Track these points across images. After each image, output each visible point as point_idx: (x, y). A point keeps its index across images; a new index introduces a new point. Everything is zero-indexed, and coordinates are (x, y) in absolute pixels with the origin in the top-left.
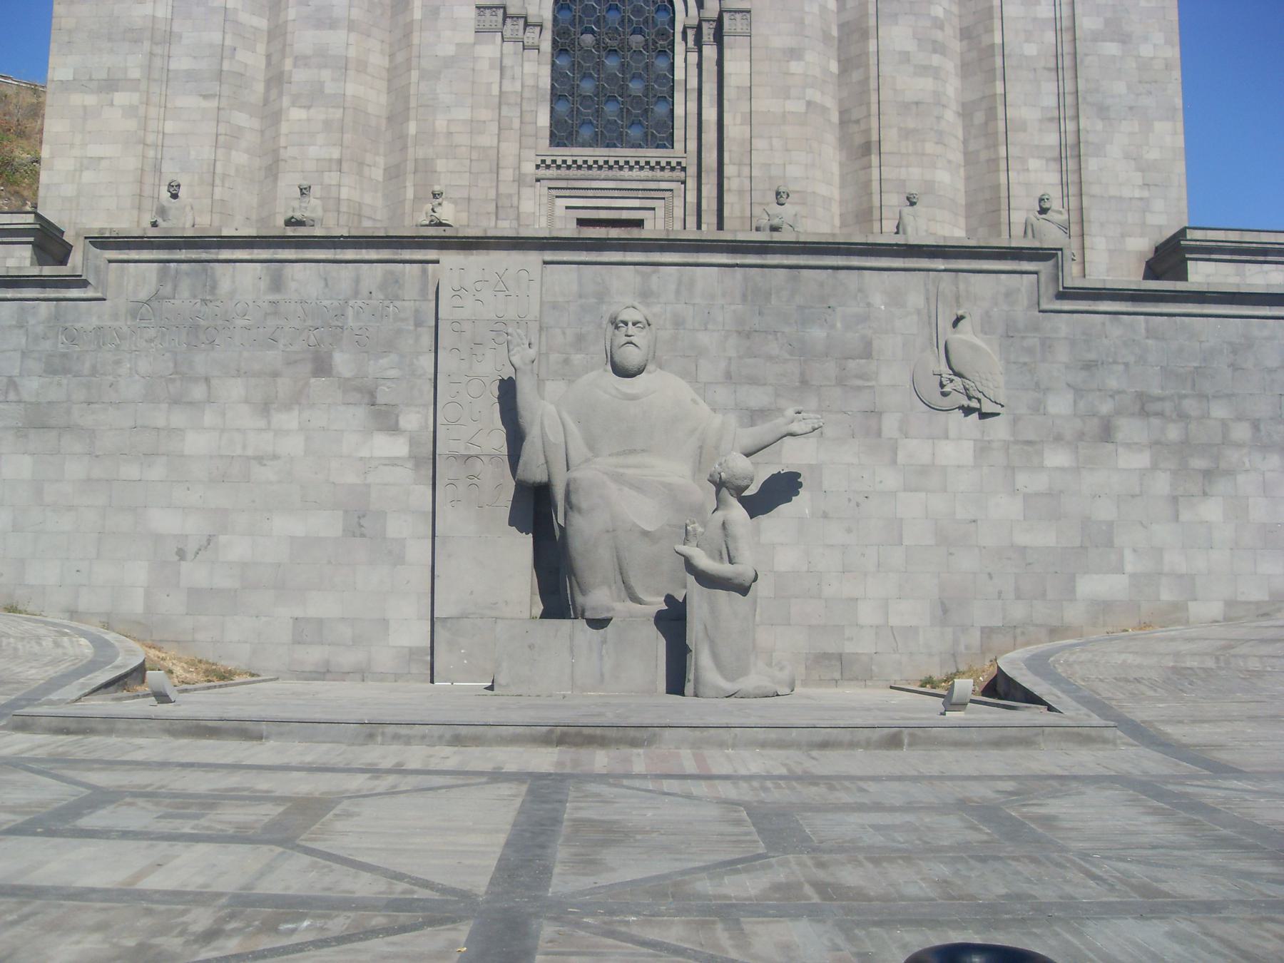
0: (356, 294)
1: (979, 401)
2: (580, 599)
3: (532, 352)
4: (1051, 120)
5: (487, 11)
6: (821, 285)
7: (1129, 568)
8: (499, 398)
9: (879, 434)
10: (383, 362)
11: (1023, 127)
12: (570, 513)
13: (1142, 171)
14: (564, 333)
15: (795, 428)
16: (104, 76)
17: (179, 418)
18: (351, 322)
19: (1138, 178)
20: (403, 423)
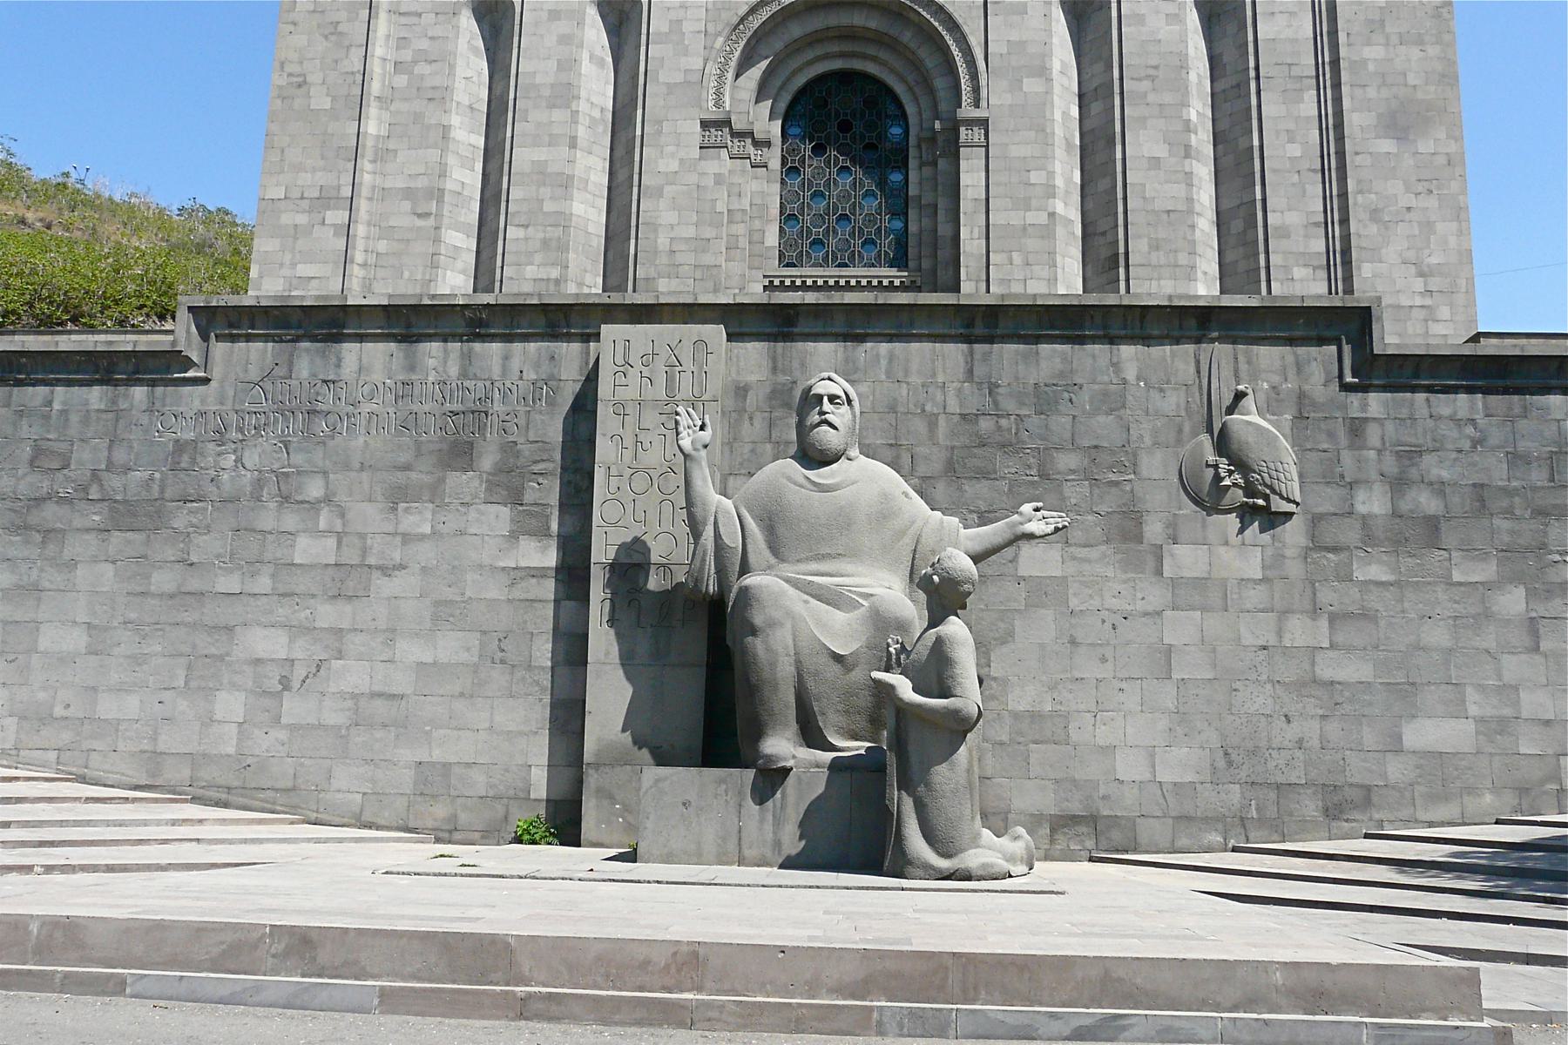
1: (1266, 498)
3: (706, 435)
4: (1316, 224)
6: (1064, 360)
7: (1473, 710)
9: (1139, 539)
11: (1285, 233)
13: (1421, 274)
15: (1035, 527)
16: (316, 194)
17: (290, 521)
19: (1419, 284)
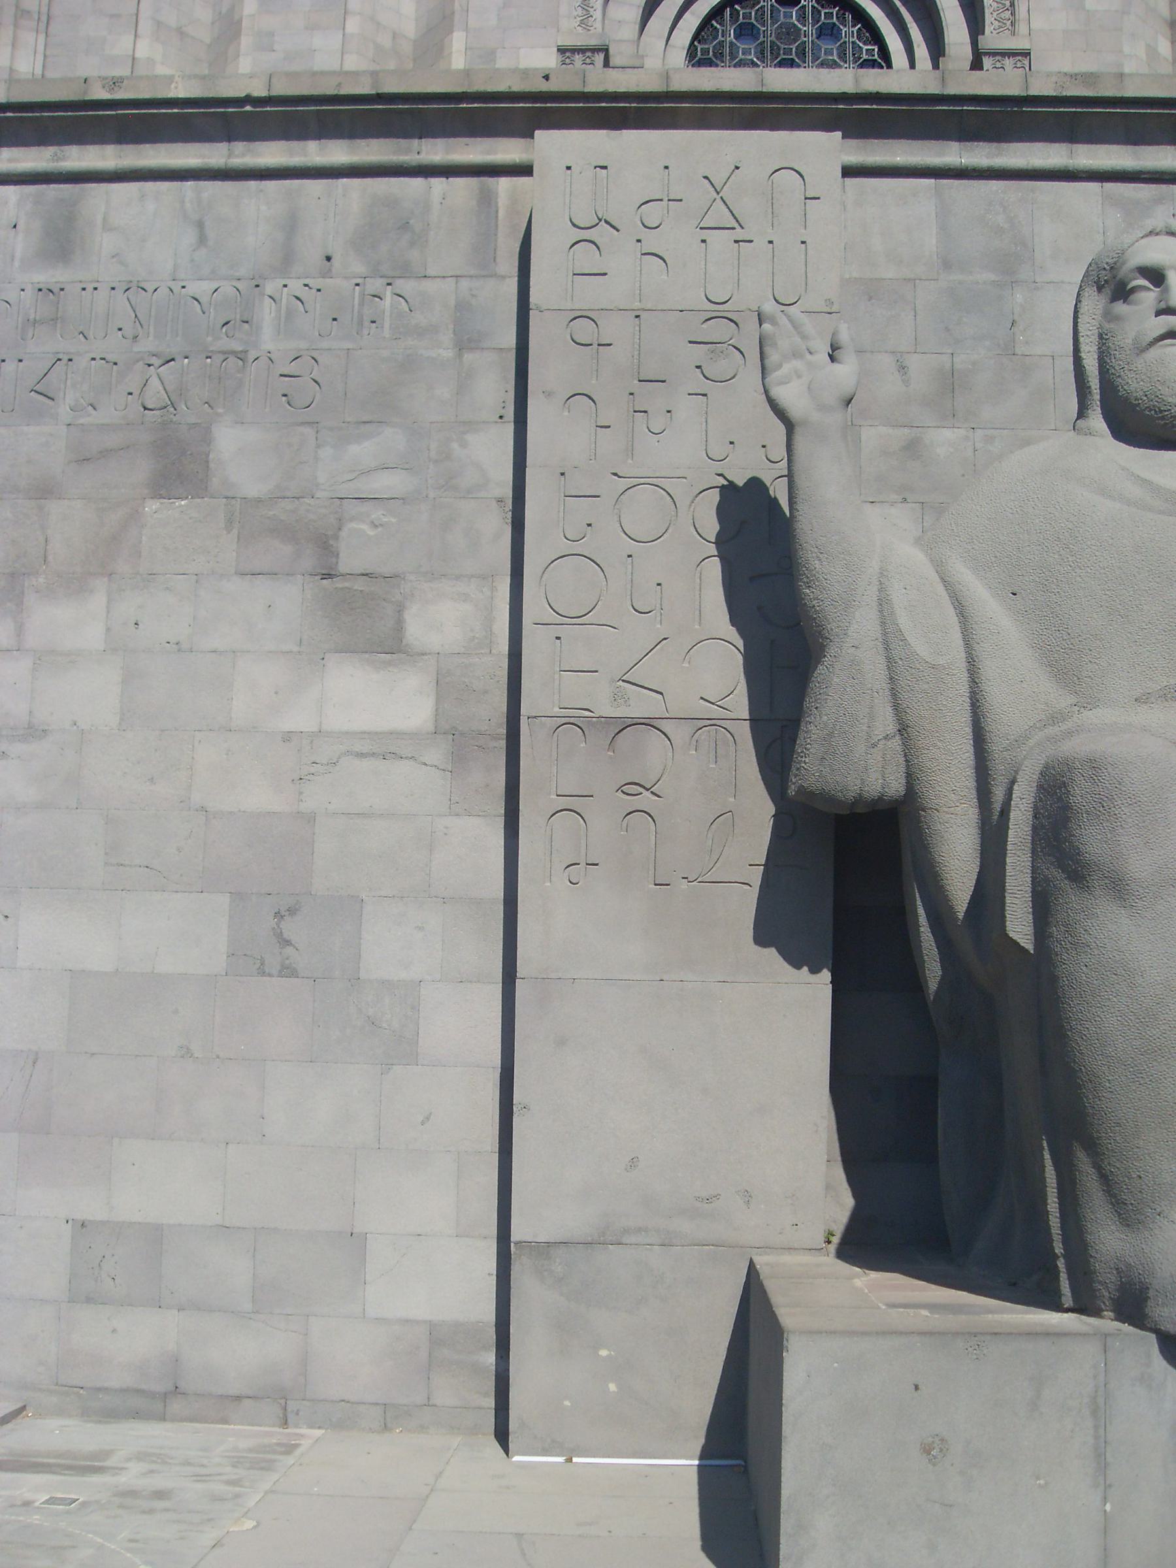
0: (286, 261)
2: (1109, 1240)
5: (578, 58)
8: (720, 542)
10: (362, 451)
12: (1070, 899)
14: (902, 368)
18: (268, 341)
20: (416, 630)
